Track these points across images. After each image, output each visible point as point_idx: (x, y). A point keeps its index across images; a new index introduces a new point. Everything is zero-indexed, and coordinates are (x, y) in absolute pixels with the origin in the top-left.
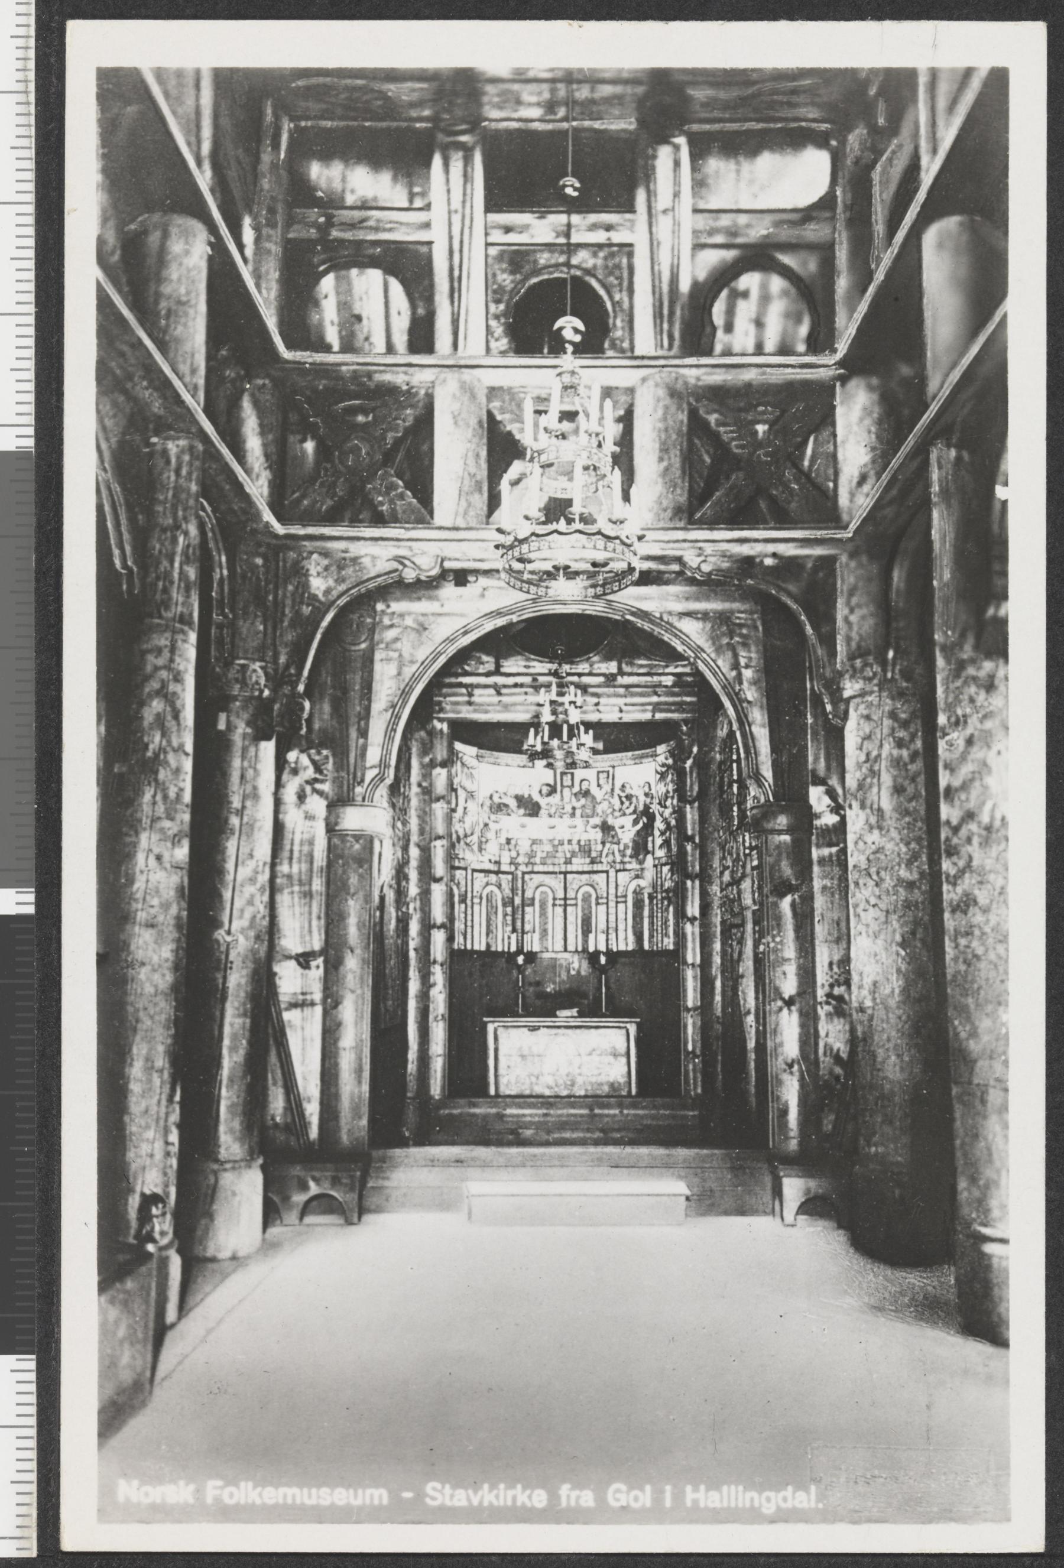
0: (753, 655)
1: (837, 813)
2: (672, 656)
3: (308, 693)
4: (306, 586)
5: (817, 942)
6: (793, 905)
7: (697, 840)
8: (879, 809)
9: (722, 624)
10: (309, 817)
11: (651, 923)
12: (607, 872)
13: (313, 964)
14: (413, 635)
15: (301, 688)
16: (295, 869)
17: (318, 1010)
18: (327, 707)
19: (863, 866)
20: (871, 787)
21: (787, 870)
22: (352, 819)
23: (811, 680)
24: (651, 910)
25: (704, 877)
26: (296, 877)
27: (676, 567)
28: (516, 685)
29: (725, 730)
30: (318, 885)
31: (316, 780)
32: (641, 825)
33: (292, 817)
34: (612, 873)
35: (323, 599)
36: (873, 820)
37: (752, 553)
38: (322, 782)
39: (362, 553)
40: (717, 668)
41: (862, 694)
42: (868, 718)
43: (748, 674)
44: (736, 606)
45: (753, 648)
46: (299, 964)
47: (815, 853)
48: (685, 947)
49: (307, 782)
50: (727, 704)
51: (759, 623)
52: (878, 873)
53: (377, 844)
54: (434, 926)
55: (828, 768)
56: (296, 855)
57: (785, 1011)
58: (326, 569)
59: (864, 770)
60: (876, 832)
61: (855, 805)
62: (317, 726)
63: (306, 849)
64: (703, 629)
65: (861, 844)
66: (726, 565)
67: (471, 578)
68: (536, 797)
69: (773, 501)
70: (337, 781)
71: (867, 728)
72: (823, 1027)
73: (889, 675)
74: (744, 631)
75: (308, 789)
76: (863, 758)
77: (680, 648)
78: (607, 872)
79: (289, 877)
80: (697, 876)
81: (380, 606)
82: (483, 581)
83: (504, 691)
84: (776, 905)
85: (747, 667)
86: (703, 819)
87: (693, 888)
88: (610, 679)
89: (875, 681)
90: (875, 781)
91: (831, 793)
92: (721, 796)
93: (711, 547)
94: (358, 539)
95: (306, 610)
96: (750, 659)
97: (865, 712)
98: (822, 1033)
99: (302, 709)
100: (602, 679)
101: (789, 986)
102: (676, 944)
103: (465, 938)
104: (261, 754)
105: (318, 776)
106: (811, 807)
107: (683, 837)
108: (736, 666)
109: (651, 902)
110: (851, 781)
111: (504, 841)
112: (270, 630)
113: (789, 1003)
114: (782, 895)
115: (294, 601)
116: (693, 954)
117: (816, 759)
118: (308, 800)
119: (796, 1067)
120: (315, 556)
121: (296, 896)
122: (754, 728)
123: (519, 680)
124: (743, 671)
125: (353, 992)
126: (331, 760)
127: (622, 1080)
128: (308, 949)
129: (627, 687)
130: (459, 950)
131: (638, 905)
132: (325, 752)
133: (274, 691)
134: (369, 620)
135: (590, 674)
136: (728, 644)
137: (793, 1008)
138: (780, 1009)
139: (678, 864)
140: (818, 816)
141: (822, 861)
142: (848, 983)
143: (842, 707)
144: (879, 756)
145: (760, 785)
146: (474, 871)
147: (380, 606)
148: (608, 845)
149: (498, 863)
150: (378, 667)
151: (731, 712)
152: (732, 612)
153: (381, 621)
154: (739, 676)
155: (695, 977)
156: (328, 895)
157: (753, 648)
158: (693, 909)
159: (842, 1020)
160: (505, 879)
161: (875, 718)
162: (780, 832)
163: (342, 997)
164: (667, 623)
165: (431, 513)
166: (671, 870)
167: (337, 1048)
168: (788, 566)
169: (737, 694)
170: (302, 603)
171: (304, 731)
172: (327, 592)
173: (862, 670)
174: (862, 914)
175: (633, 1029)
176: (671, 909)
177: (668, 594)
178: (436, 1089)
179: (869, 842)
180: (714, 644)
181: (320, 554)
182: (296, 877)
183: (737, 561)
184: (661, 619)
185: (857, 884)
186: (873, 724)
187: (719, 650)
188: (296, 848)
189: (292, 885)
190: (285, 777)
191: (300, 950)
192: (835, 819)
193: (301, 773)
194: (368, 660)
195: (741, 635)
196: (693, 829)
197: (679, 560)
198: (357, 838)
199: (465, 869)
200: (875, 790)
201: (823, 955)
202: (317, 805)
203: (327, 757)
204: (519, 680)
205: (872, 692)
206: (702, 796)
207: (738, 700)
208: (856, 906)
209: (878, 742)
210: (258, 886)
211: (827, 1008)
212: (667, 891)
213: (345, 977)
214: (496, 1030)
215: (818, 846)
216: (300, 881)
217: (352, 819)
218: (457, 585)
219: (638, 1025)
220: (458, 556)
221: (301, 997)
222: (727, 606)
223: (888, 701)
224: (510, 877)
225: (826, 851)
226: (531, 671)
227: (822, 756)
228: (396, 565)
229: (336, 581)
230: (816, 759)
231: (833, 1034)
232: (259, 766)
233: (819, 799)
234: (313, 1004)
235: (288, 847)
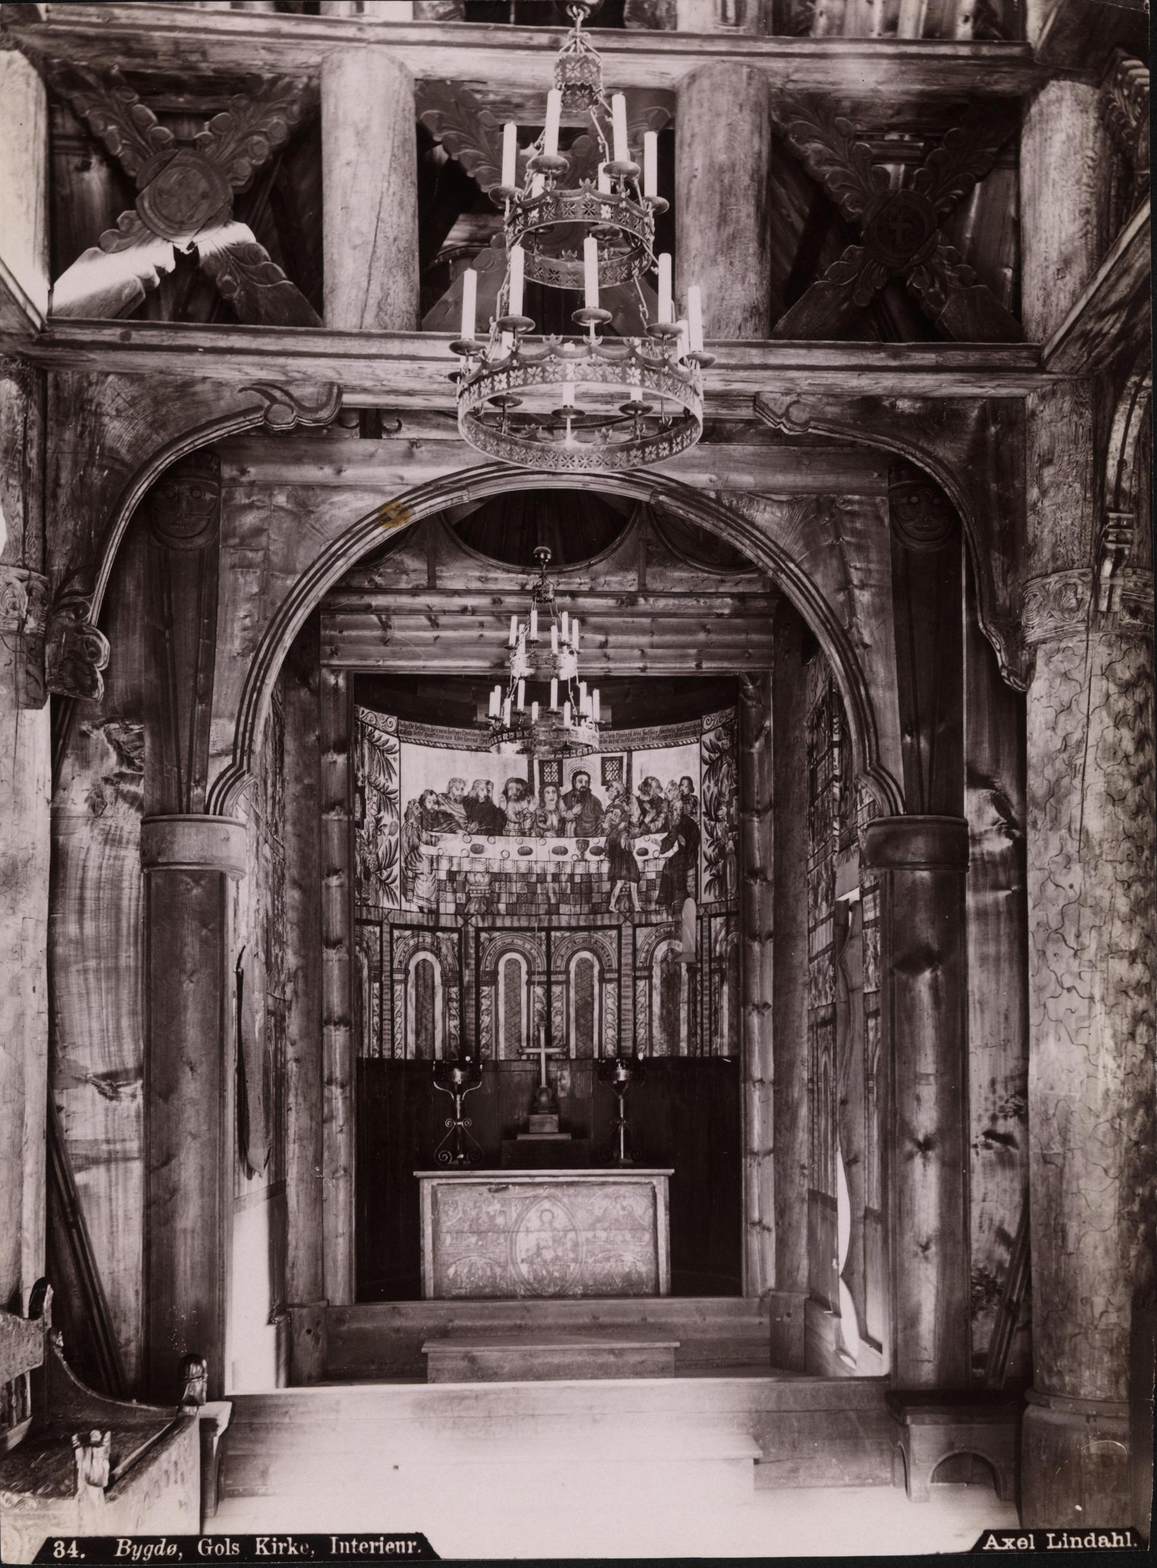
0: (872, 566)
1: (1009, 835)
2: (733, 562)
3: (104, 623)
4: (98, 433)
5: (972, 1047)
6: (934, 987)
7: (770, 877)
8: (1083, 830)
9: (817, 512)
10: (112, 839)
11: (692, 1013)
12: (618, 928)
13: (125, 1091)
14: (287, 523)
15: (93, 614)
16: (89, 928)
17: (137, 1167)
18: (137, 646)
19: (1054, 924)
20: (1068, 793)
21: (926, 932)
22: (189, 844)
23: (971, 610)
24: (693, 992)
25: (784, 938)
26: (91, 945)
27: (746, 412)
28: (464, 610)
29: (821, 690)
30: (128, 957)
31: (121, 776)
33: (83, 838)
34: (627, 931)
35: (128, 458)
36: (1072, 847)
37: (878, 390)
38: (133, 779)
39: (199, 374)
40: (811, 589)
41: (1060, 634)
42: (1066, 676)
43: (864, 597)
44: (844, 480)
45: (873, 556)
46: (102, 1092)
47: (971, 900)
48: (748, 1052)
49: (107, 780)
50: (829, 649)
51: (884, 512)
52: (1078, 936)
53: (231, 885)
54: (328, 1022)
55: (996, 760)
56: (90, 905)
57: (918, 1161)
58: (133, 402)
59: (1059, 764)
60: (1077, 868)
61: (1043, 821)
62: (120, 683)
63: (106, 894)
64: (791, 518)
65: (1051, 887)
66: (831, 411)
67: (391, 425)
68: (497, 800)
69: (912, 302)
70: (159, 778)
71: (1065, 692)
72: (980, 1184)
73: (1103, 606)
74: (858, 525)
75: (109, 791)
76: (1058, 744)
77: (749, 553)
78: (618, 928)
79: (80, 943)
80: (769, 936)
81: (228, 472)
82: (410, 432)
83: (443, 620)
84: (907, 988)
85: (863, 586)
86: (782, 843)
87: (762, 953)
88: (627, 600)
89: (1081, 615)
90: (1077, 782)
91: (1000, 802)
92: (812, 804)
93: (814, 375)
94: (191, 349)
95: (97, 476)
96: (868, 571)
97: (1063, 667)
98: (977, 1192)
99: (97, 654)
100: (611, 602)
101: (926, 1118)
102: (734, 1046)
103: (380, 1040)
104: (24, 732)
105: (125, 769)
106: (966, 824)
107: (748, 872)
108: (845, 585)
109: (692, 978)
110: (1037, 784)
111: (443, 875)
112: (34, 513)
113: (925, 1146)
114: (917, 970)
115: (75, 463)
116: (761, 1065)
117: (976, 745)
118: (108, 811)
119: (933, 1249)
120: (111, 378)
121: (91, 977)
122: (872, 692)
123: (470, 601)
124: (857, 592)
125: (194, 1137)
126: (148, 742)
127: (644, 1269)
128: (120, 1068)
129: (654, 615)
130: (371, 1060)
131: (671, 983)
132: (136, 728)
133: (47, 619)
134: (208, 496)
135: (592, 593)
136: (831, 547)
137: (931, 1154)
138: (910, 1156)
139: (739, 915)
140: (977, 839)
141: (982, 914)
142: (1022, 1114)
143: (1025, 657)
144: (1084, 740)
145: (882, 787)
146: (394, 926)
147: (228, 472)
148: (620, 884)
149: (435, 913)
150: (227, 578)
151: (836, 661)
152: (840, 491)
153: (231, 497)
154: (851, 600)
155: (764, 1102)
156: (148, 974)
157: (873, 556)
158: (763, 989)
159: (1009, 1173)
161: (1079, 676)
162: (915, 866)
163: (178, 1145)
164: (730, 509)
165: (318, 304)
166: (727, 924)
167: (173, 1231)
168: (939, 415)
169: (845, 633)
170: (90, 463)
171: (100, 693)
172: (136, 445)
173: (1059, 593)
174: (1051, 1003)
175: (662, 1187)
176: (726, 988)
177: (730, 458)
178: (339, 1289)
179: (1066, 885)
180: (807, 546)
181: (121, 375)
182: (91, 945)
183: (851, 404)
184: (718, 501)
185: (1043, 953)
186: (1074, 687)
187: (815, 555)
188: (89, 894)
189: (85, 959)
190: (67, 767)
191: (101, 1069)
192: (1007, 843)
193: (95, 763)
194: (207, 568)
195: (854, 532)
196: (763, 858)
197: (755, 399)
198: (197, 877)
200: (1076, 798)
201: (982, 1067)
202: (128, 821)
203: (140, 737)
204: (470, 601)
205: (1076, 633)
206: (780, 803)
207: (846, 643)
208: (1040, 989)
209: (1081, 717)
210: (28, 960)
211: (984, 1153)
212: (721, 958)
213: (181, 1111)
214: (434, 1194)
215: (976, 889)
216: (98, 950)
217: (189, 844)
218: (364, 435)
219: (671, 1179)
220: (368, 384)
221: (104, 1147)
222: (830, 480)
223: (1103, 650)
224: (455, 936)
225: (989, 897)
226: (492, 586)
227: (986, 737)
228: (257, 398)
229: (151, 425)
230: (976, 745)
231: (993, 1197)
232: (20, 755)
233: (980, 813)
234: (127, 1159)
235: (75, 892)
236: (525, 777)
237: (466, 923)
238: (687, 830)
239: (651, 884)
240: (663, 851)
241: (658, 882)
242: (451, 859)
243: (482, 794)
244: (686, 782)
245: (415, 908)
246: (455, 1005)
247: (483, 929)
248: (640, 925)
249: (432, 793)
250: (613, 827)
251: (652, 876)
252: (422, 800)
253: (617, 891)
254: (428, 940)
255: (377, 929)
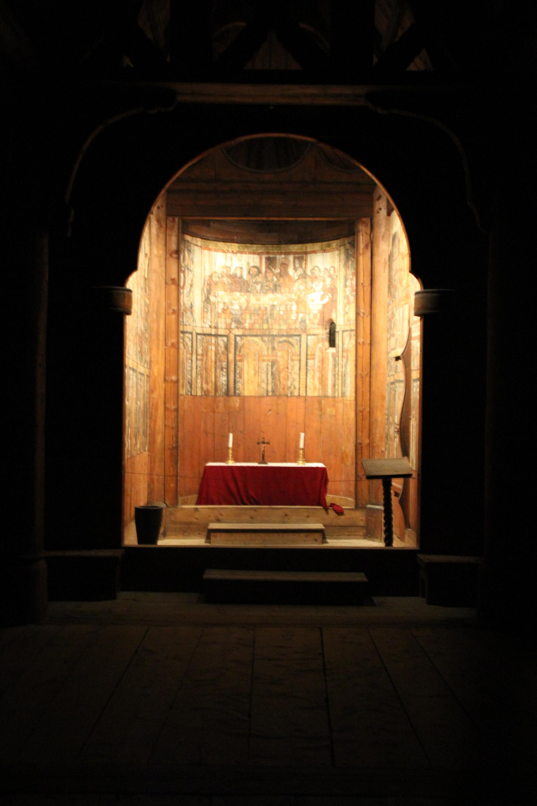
32: (326, 300)
34: (304, 337)
68: (245, 277)
78: (299, 336)
111: (220, 311)
146: (197, 334)
148: (301, 315)
149: (216, 328)
160: (221, 341)
199: (191, 333)
224: (225, 339)
236: (258, 264)
237: (230, 332)
238: (333, 290)
239: (315, 316)
240: (321, 300)
241: (319, 315)
242: (224, 303)
243: (239, 274)
244: (332, 269)
245: (208, 326)
246: (225, 370)
247: (238, 336)
248: (310, 335)
249: (215, 272)
250: (299, 290)
251: (316, 312)
252: (211, 276)
253: (299, 319)
254: (213, 341)
255: (190, 336)
